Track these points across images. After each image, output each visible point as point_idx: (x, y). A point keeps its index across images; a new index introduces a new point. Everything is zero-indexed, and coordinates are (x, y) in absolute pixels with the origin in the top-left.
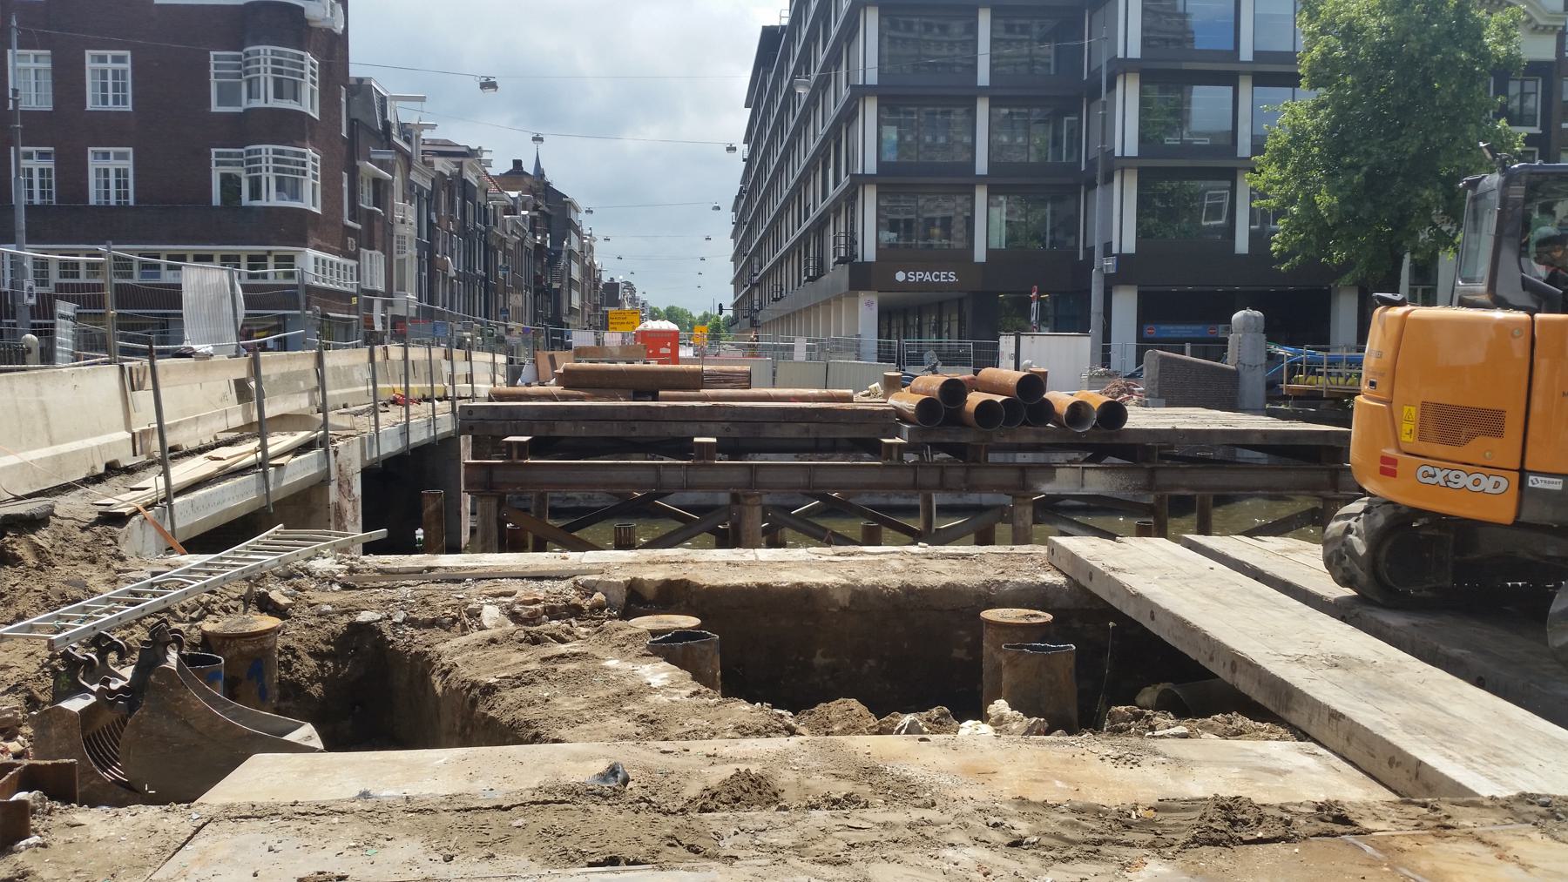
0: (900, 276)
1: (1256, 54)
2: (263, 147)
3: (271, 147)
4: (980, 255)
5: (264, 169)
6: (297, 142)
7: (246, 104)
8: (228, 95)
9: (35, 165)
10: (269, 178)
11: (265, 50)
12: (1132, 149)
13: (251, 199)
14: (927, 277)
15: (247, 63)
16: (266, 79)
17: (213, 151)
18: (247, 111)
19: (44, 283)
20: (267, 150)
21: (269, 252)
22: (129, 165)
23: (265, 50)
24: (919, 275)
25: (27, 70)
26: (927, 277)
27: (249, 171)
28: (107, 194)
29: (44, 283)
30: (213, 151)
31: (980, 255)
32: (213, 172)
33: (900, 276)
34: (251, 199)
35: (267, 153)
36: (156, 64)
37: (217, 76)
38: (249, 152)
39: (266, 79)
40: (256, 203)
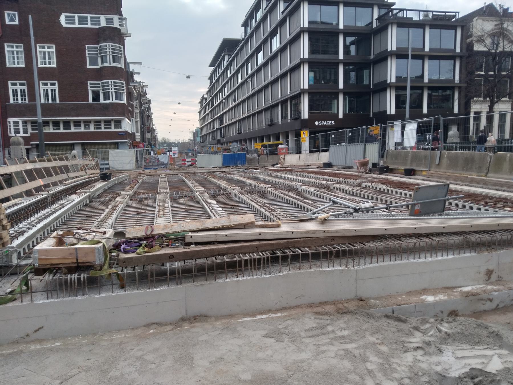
1: (430, 49)
2: (110, 81)
3: (113, 81)
4: (341, 116)
5: (110, 89)
6: (121, 79)
7: (100, 65)
8: (94, 61)
9: (18, 87)
10: (112, 92)
11: (109, 45)
12: (394, 80)
13: (104, 100)
15: (101, 50)
16: (110, 55)
17: (89, 82)
18: (101, 68)
19: (27, 133)
20: (111, 82)
21: (112, 119)
22: (56, 87)
23: (109, 45)
27: (103, 90)
28: (48, 99)
29: (27, 133)
30: (89, 82)
31: (341, 116)
32: (89, 90)
33: (317, 123)
34: (104, 100)
35: (111, 83)
36: (64, 50)
37: (89, 54)
38: (103, 83)
39: (110, 55)
40: (107, 102)
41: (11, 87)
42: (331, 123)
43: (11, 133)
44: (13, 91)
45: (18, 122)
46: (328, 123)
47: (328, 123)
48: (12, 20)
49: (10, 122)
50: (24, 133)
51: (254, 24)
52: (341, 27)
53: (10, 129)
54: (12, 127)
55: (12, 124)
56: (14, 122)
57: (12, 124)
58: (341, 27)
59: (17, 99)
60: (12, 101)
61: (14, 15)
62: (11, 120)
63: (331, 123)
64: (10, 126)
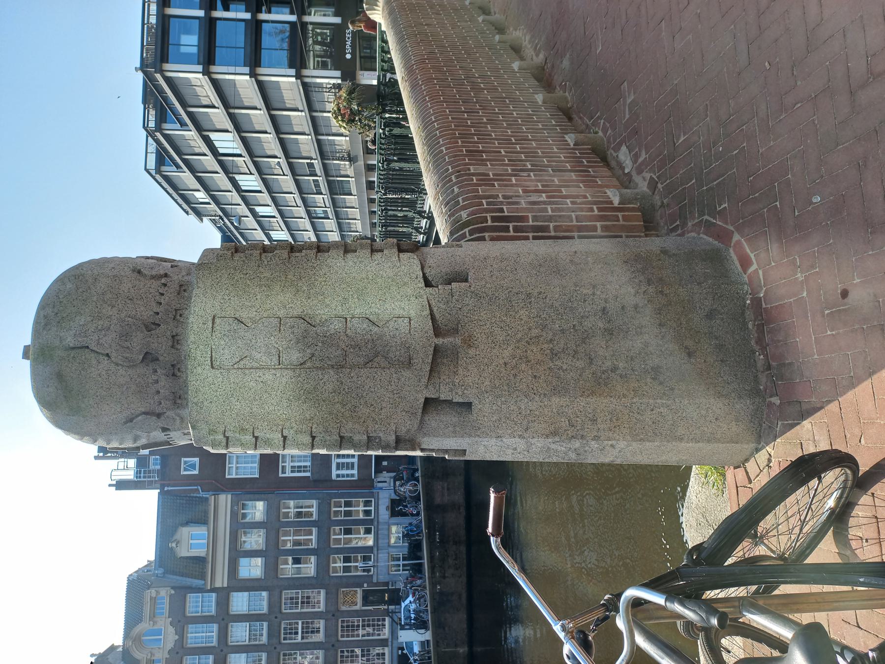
0: (348, 56)
4: (337, 20)
14: (349, 43)
24: (348, 47)
25: (237, 468)
26: (349, 43)
31: (337, 20)
33: (348, 56)
41: (288, 474)
42: (349, 33)
43: (353, 475)
44: (292, 472)
45: (338, 464)
46: (349, 38)
47: (349, 38)
48: (193, 466)
49: (338, 476)
50: (353, 468)
51: (201, 196)
52: (201, 13)
53: (348, 475)
54: (345, 472)
55: (340, 472)
56: (338, 468)
57: (340, 472)
58: (201, 13)
59: (305, 467)
60: (308, 474)
61: (185, 462)
62: (334, 472)
63: (349, 33)
64: (343, 476)
